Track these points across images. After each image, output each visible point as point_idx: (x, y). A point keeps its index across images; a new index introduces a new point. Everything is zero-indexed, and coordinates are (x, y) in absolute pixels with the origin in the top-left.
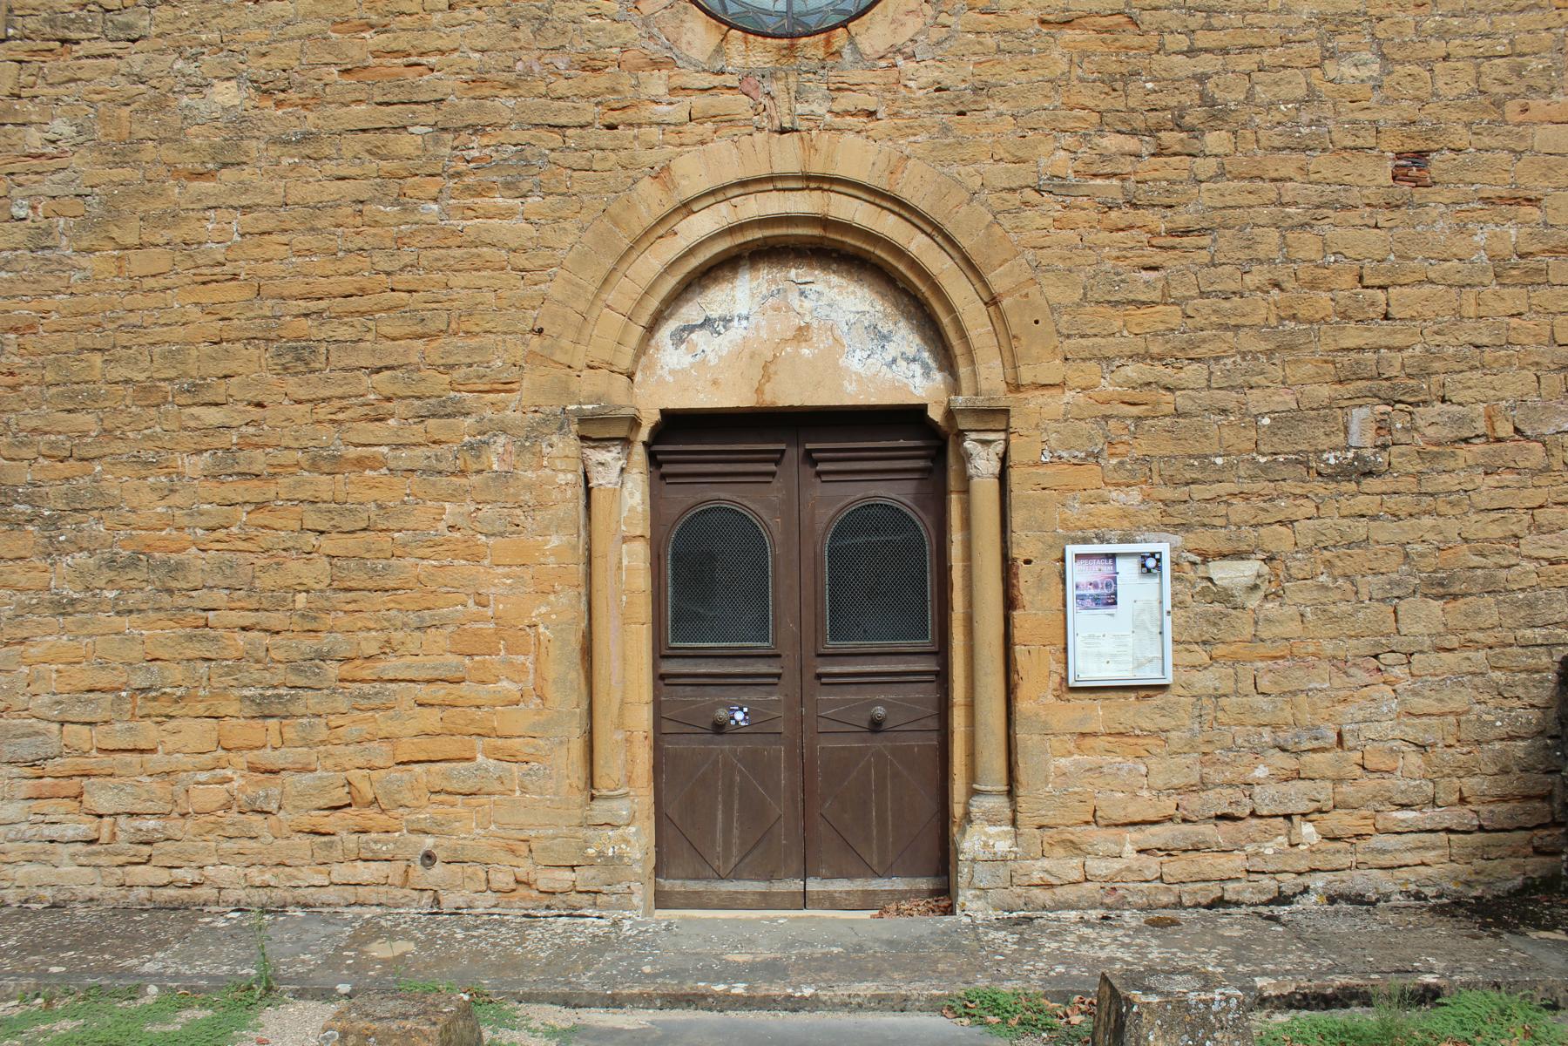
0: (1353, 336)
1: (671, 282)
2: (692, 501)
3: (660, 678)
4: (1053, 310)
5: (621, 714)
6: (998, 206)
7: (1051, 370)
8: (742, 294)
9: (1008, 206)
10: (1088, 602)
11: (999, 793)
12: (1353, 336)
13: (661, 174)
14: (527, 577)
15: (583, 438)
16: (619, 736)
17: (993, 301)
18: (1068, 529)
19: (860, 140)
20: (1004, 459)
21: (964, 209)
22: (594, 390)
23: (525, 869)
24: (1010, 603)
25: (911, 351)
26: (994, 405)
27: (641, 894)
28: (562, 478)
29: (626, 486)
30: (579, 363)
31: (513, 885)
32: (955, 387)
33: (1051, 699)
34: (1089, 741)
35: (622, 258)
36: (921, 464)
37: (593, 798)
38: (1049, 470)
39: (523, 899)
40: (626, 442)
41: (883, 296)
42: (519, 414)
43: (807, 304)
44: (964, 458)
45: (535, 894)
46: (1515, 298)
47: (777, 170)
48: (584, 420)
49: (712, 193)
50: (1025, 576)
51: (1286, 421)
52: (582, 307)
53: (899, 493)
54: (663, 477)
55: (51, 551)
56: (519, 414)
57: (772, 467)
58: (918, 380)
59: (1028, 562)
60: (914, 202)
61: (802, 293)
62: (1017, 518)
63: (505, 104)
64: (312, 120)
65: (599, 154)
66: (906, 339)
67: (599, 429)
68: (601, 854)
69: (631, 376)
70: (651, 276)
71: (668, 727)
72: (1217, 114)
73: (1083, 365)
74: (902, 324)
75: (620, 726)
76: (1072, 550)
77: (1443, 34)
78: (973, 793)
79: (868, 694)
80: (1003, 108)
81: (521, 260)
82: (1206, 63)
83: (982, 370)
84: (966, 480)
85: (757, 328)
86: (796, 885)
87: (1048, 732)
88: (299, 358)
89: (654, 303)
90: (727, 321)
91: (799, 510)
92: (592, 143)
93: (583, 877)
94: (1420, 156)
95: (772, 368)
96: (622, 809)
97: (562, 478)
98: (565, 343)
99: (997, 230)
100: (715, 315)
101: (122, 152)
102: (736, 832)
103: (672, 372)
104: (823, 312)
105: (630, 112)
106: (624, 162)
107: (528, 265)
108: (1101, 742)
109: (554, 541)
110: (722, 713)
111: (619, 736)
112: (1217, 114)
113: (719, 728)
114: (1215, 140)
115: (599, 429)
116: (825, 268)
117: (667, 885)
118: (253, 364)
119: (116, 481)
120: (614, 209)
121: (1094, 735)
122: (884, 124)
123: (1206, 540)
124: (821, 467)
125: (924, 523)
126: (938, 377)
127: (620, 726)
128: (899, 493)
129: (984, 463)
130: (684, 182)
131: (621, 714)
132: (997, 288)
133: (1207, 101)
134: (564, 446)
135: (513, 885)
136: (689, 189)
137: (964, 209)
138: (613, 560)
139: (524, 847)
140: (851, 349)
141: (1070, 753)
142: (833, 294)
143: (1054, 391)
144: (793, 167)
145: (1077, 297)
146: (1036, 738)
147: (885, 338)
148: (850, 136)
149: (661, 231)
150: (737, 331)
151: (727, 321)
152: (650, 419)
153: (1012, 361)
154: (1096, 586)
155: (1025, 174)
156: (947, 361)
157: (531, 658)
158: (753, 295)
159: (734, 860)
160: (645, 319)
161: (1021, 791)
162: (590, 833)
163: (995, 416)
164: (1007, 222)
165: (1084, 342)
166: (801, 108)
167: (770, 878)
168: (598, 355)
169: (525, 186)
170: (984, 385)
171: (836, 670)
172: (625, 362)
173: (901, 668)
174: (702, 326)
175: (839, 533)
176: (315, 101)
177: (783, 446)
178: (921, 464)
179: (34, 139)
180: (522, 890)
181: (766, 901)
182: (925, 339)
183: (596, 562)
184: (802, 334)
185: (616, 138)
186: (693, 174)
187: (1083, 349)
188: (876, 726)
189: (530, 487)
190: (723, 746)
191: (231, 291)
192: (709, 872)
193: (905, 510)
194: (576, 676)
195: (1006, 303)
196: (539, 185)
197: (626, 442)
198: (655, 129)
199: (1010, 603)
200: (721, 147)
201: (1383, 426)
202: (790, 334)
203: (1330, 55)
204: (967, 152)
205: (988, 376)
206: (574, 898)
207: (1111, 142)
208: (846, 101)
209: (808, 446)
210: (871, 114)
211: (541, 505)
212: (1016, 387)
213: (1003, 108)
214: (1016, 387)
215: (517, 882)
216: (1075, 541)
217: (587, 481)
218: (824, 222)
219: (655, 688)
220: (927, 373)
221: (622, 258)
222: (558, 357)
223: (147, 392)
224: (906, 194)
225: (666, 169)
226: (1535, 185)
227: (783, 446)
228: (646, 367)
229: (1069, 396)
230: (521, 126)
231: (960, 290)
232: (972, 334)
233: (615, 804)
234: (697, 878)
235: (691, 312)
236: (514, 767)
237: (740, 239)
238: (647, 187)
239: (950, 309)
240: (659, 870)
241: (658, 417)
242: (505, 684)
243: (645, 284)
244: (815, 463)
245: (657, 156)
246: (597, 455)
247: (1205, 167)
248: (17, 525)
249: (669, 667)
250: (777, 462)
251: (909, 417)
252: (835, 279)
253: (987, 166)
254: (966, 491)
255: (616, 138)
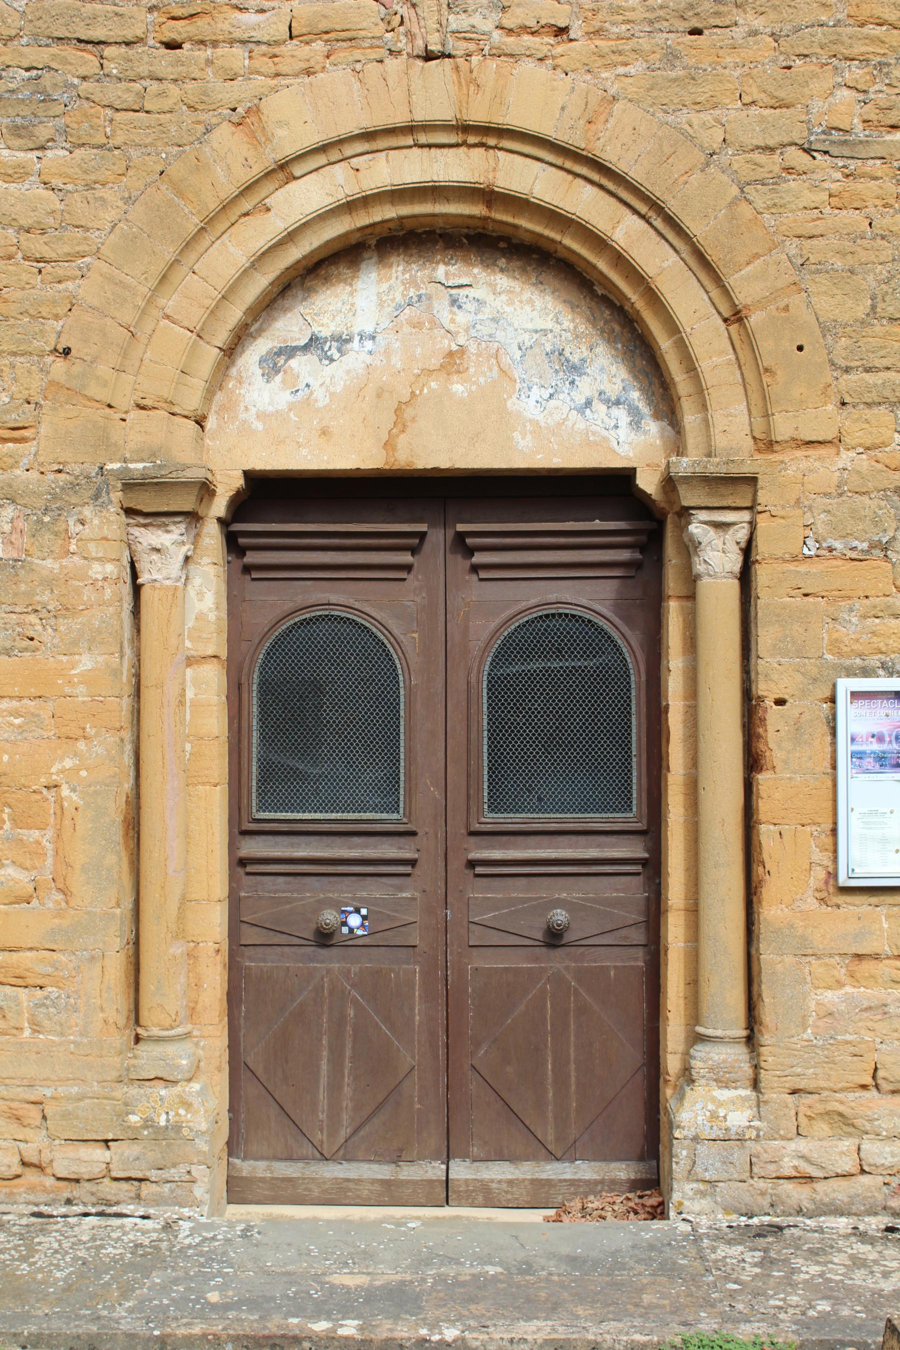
1: (261, 282)
2: (289, 606)
3: (240, 864)
4: (825, 330)
5: (181, 917)
6: (747, 173)
7: (821, 420)
8: (366, 300)
9: (761, 174)
10: (869, 762)
11: (734, 1040)
13: (247, 118)
14: (45, 715)
15: (130, 512)
16: (178, 949)
17: (736, 317)
18: (840, 654)
19: (543, 72)
20: (747, 551)
21: (696, 178)
22: (149, 442)
23: (35, 1144)
24: (753, 762)
25: (614, 390)
26: (735, 470)
27: (207, 1182)
28: (97, 570)
29: (193, 582)
30: (124, 400)
31: (17, 1169)
32: (677, 444)
33: (811, 903)
34: (867, 967)
35: (188, 245)
36: (624, 555)
37: (138, 1039)
38: (815, 568)
39: (32, 1189)
40: (193, 517)
41: (573, 307)
42: (34, 475)
43: (462, 318)
44: (689, 549)
45: (50, 1182)
47: (420, 116)
48: (129, 486)
49: (323, 149)
50: (775, 725)
52: (128, 316)
53: (593, 598)
54: (247, 569)
56: (34, 475)
57: (406, 558)
58: (624, 433)
59: (780, 702)
60: (621, 166)
61: (454, 302)
62: (765, 637)
65: (154, 86)
66: (607, 370)
67: (150, 500)
68: (148, 1123)
69: (200, 422)
70: (230, 272)
71: (250, 935)
73: (868, 413)
74: (602, 349)
75: (180, 934)
76: (846, 685)
78: (697, 1039)
79: (543, 890)
80: (758, 23)
81: (37, 245)
83: (718, 419)
84: (691, 580)
85: (387, 352)
86: (434, 1170)
87: (806, 952)
89: (235, 314)
90: (343, 341)
91: (441, 621)
92: (143, 70)
93: (122, 1157)
95: (409, 412)
96: (180, 1056)
97: (97, 570)
98: (103, 370)
99: (745, 210)
100: (325, 333)
102: (347, 1091)
103: (262, 416)
104: (484, 330)
105: (200, 22)
106: (192, 99)
107: (48, 253)
108: (886, 968)
109: (86, 663)
110: (329, 917)
111: (178, 949)
113: (325, 938)
115: (150, 500)
116: (489, 264)
117: (246, 1167)
120: (176, 170)
121: (876, 957)
122: (579, 47)
124: (479, 558)
125: (629, 641)
126: (653, 427)
127: (180, 934)
128: (593, 598)
129: (718, 556)
130: (281, 133)
131: (181, 917)
132: (742, 297)
134: (103, 522)
135: (17, 1169)
136: (289, 142)
137: (696, 178)
138: (172, 690)
139: (34, 1113)
141: (840, 984)
142: (498, 303)
143: (822, 451)
144: (444, 112)
145: (862, 309)
146: (789, 960)
147: (576, 369)
148: (528, 66)
149: (246, 205)
150: (357, 357)
151: (343, 341)
152: (228, 484)
153: (763, 406)
154: (880, 739)
155: (787, 126)
156: (666, 405)
157: (50, 833)
158: (381, 304)
159: (343, 1133)
160: (222, 337)
161: (766, 1038)
162: (133, 1091)
163: (736, 486)
164: (759, 197)
165: (870, 378)
166: (456, 22)
167: (396, 1158)
168: (153, 388)
169: (43, 132)
170: (720, 442)
171: (497, 854)
172: (192, 401)
173: (593, 853)
174: (306, 348)
175: (504, 654)
177: (422, 527)
178: (624, 555)
180: (31, 1176)
181: (390, 1194)
182: (634, 371)
183: (147, 694)
184: (453, 362)
185: (179, 62)
186: (296, 120)
187: (869, 389)
188: (554, 938)
189: (49, 583)
190: (330, 963)
192: (308, 1150)
193: (601, 622)
194: (116, 860)
195: (755, 319)
196: (65, 131)
197: (193, 517)
198: (238, 51)
199: (753, 762)
200: (336, 79)
202: (435, 362)
204: (703, 92)
205: (726, 430)
206: (108, 1188)
209: (461, 527)
210: (561, 31)
211: (67, 610)
212: (767, 444)
213: (758, 23)
214: (767, 444)
215: (24, 1164)
216: (850, 672)
217: (135, 575)
218: (488, 196)
219: (232, 878)
220: (636, 423)
221: (188, 245)
222: (94, 391)
224: (610, 156)
225: (254, 111)
227: (422, 527)
228: (223, 408)
229: (846, 458)
230: (36, 40)
231: (688, 300)
232: (704, 365)
233: (170, 1049)
234: (290, 1158)
235: (289, 326)
236: (23, 993)
237: (363, 219)
238: (225, 137)
239: (673, 328)
240: (233, 1147)
241: (240, 482)
242: (11, 871)
243: (222, 284)
244: (470, 552)
245: (239, 92)
246: (149, 537)
249: (253, 848)
250: (414, 550)
251: (608, 488)
252: (502, 281)
253: (733, 112)
254: (691, 596)
255: (179, 62)
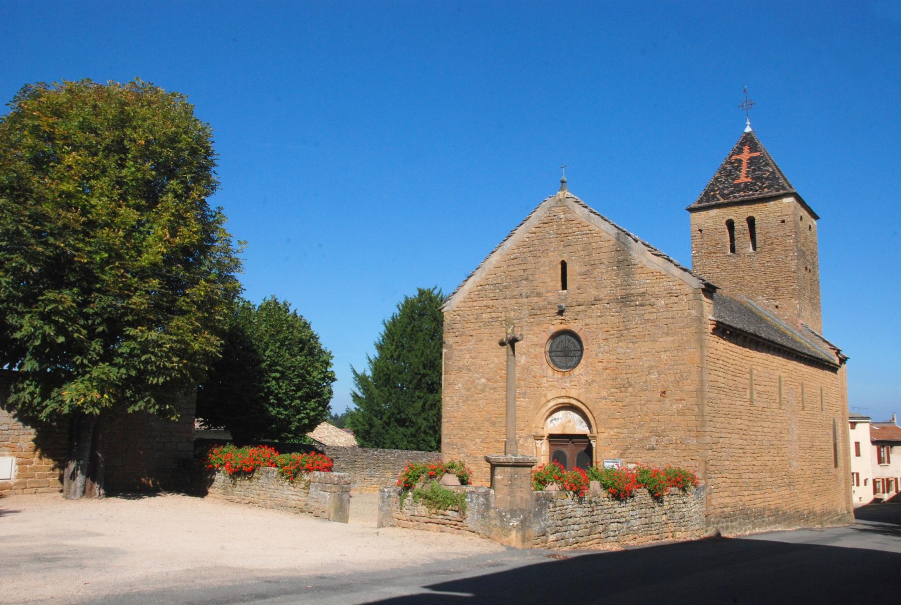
0: (652, 424)
7: (602, 430)
12: (652, 424)
13: (545, 396)
46: (681, 418)
51: (641, 440)
55: (459, 453)
63: (522, 383)
64: (495, 385)
66: (584, 424)
72: (630, 385)
77: (669, 369)
82: (629, 376)
88: (494, 424)
91: (570, 451)
94: (664, 392)
101: (468, 390)
112: (630, 385)
114: (630, 389)
118: (487, 424)
119: (468, 443)
123: (628, 460)
133: (629, 382)
140: (575, 425)
150: (560, 421)
152: (546, 435)
172: (541, 426)
176: (495, 382)
179: (456, 387)
184: (570, 421)
186: (550, 397)
191: (484, 413)
200: (554, 391)
201: (657, 441)
203: (649, 374)
207: (613, 390)
208: (573, 383)
223: (472, 428)
226: (685, 397)
247: (628, 394)
248: (454, 449)
251: (584, 436)
